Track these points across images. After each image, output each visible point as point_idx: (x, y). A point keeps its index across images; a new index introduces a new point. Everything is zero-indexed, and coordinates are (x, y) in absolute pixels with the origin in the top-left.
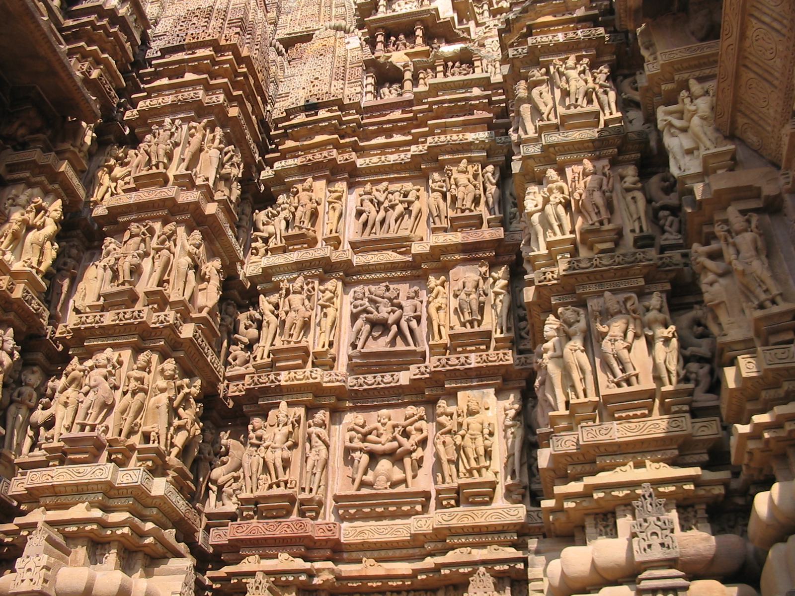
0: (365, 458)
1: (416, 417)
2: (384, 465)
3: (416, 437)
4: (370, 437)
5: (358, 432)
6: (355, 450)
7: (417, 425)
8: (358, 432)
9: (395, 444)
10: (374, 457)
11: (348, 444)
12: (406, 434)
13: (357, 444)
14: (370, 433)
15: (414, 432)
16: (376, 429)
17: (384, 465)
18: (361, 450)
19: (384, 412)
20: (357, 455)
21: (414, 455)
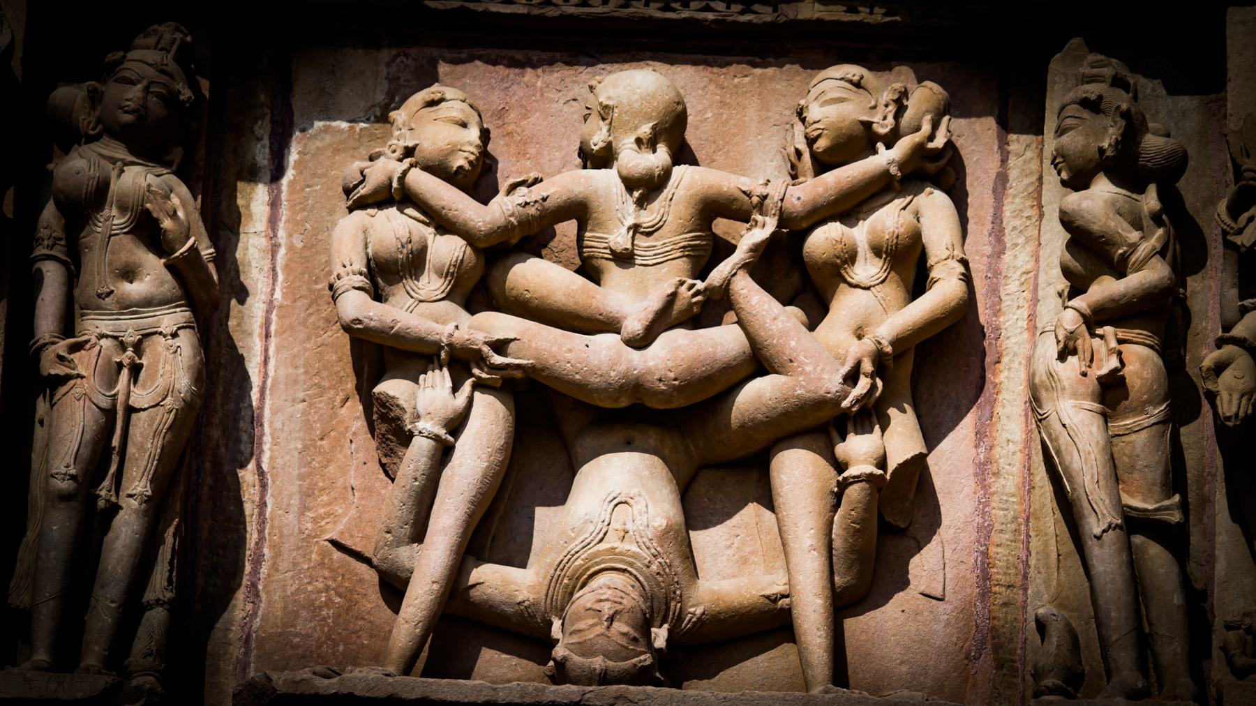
0: (489, 421)
1: (885, 158)
2: (618, 498)
3: (871, 314)
4: (537, 275)
5: (443, 224)
6: (413, 356)
7: (889, 219)
8: (443, 224)
9: (724, 340)
10: (554, 426)
11: (355, 305)
12: (802, 280)
13: (423, 311)
14: (530, 237)
15: (867, 269)
16: (579, 211)
17: (618, 498)
18: (460, 362)
19: (637, 86)
20: (427, 397)
21: (859, 449)
